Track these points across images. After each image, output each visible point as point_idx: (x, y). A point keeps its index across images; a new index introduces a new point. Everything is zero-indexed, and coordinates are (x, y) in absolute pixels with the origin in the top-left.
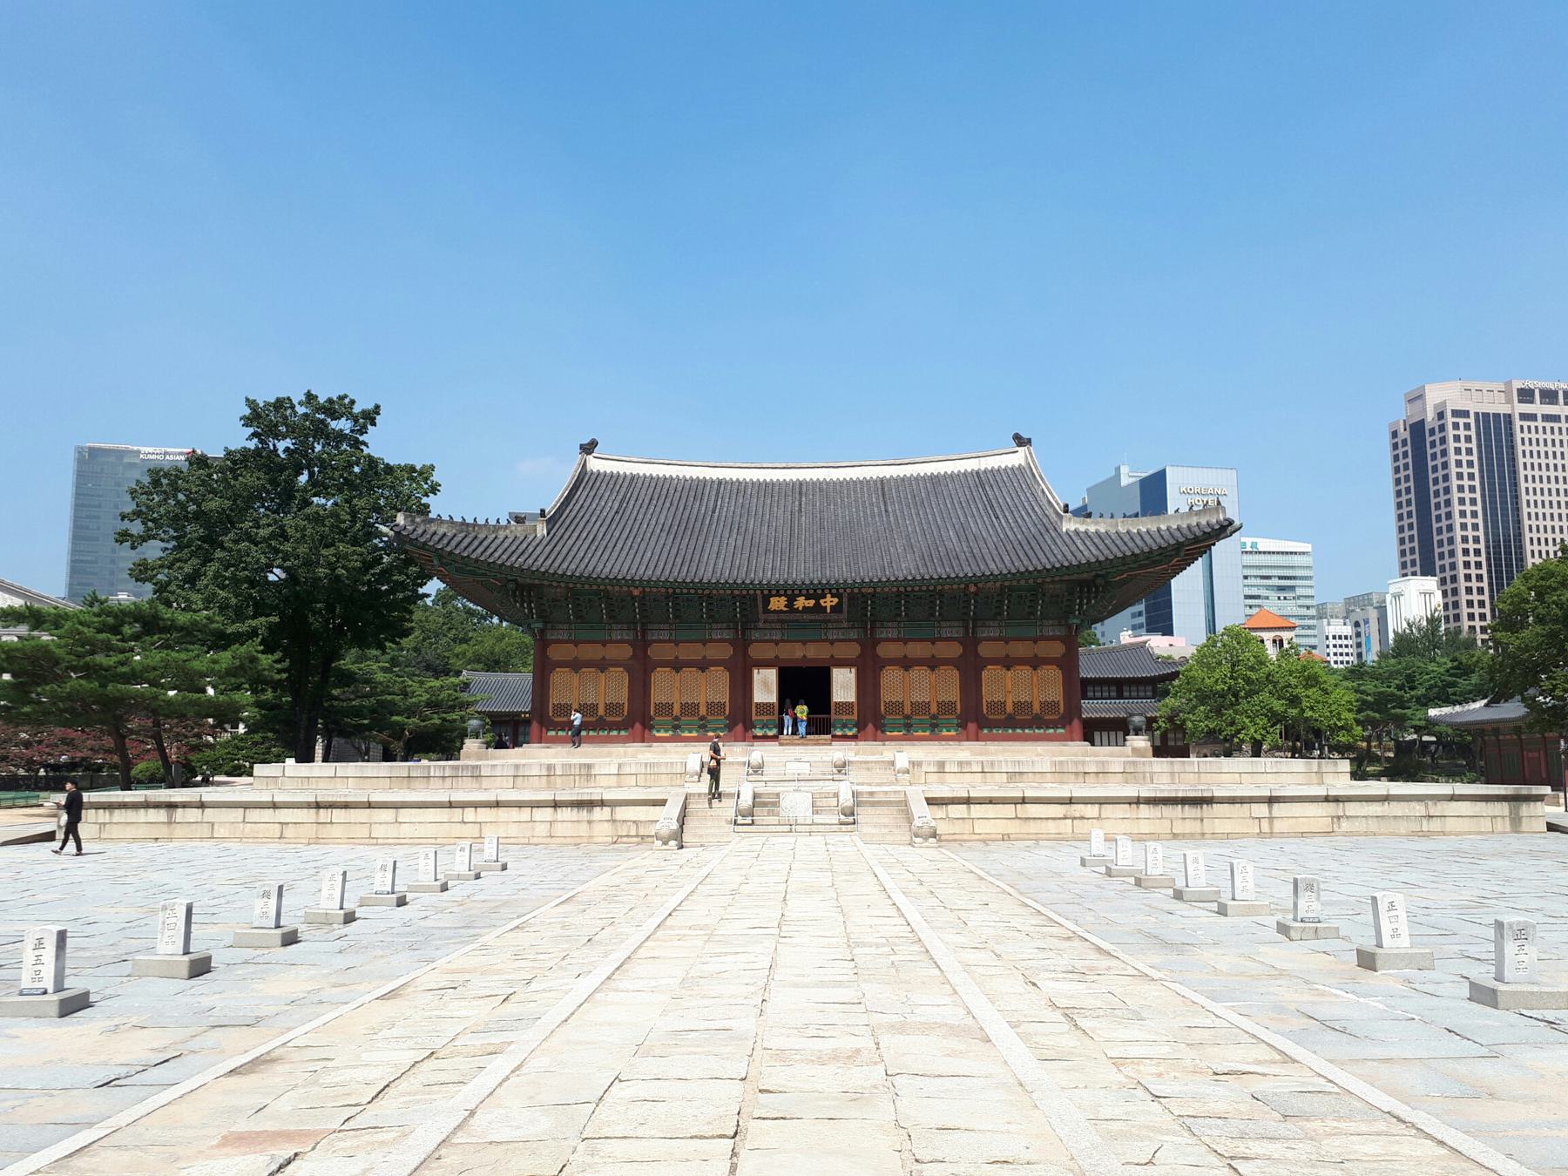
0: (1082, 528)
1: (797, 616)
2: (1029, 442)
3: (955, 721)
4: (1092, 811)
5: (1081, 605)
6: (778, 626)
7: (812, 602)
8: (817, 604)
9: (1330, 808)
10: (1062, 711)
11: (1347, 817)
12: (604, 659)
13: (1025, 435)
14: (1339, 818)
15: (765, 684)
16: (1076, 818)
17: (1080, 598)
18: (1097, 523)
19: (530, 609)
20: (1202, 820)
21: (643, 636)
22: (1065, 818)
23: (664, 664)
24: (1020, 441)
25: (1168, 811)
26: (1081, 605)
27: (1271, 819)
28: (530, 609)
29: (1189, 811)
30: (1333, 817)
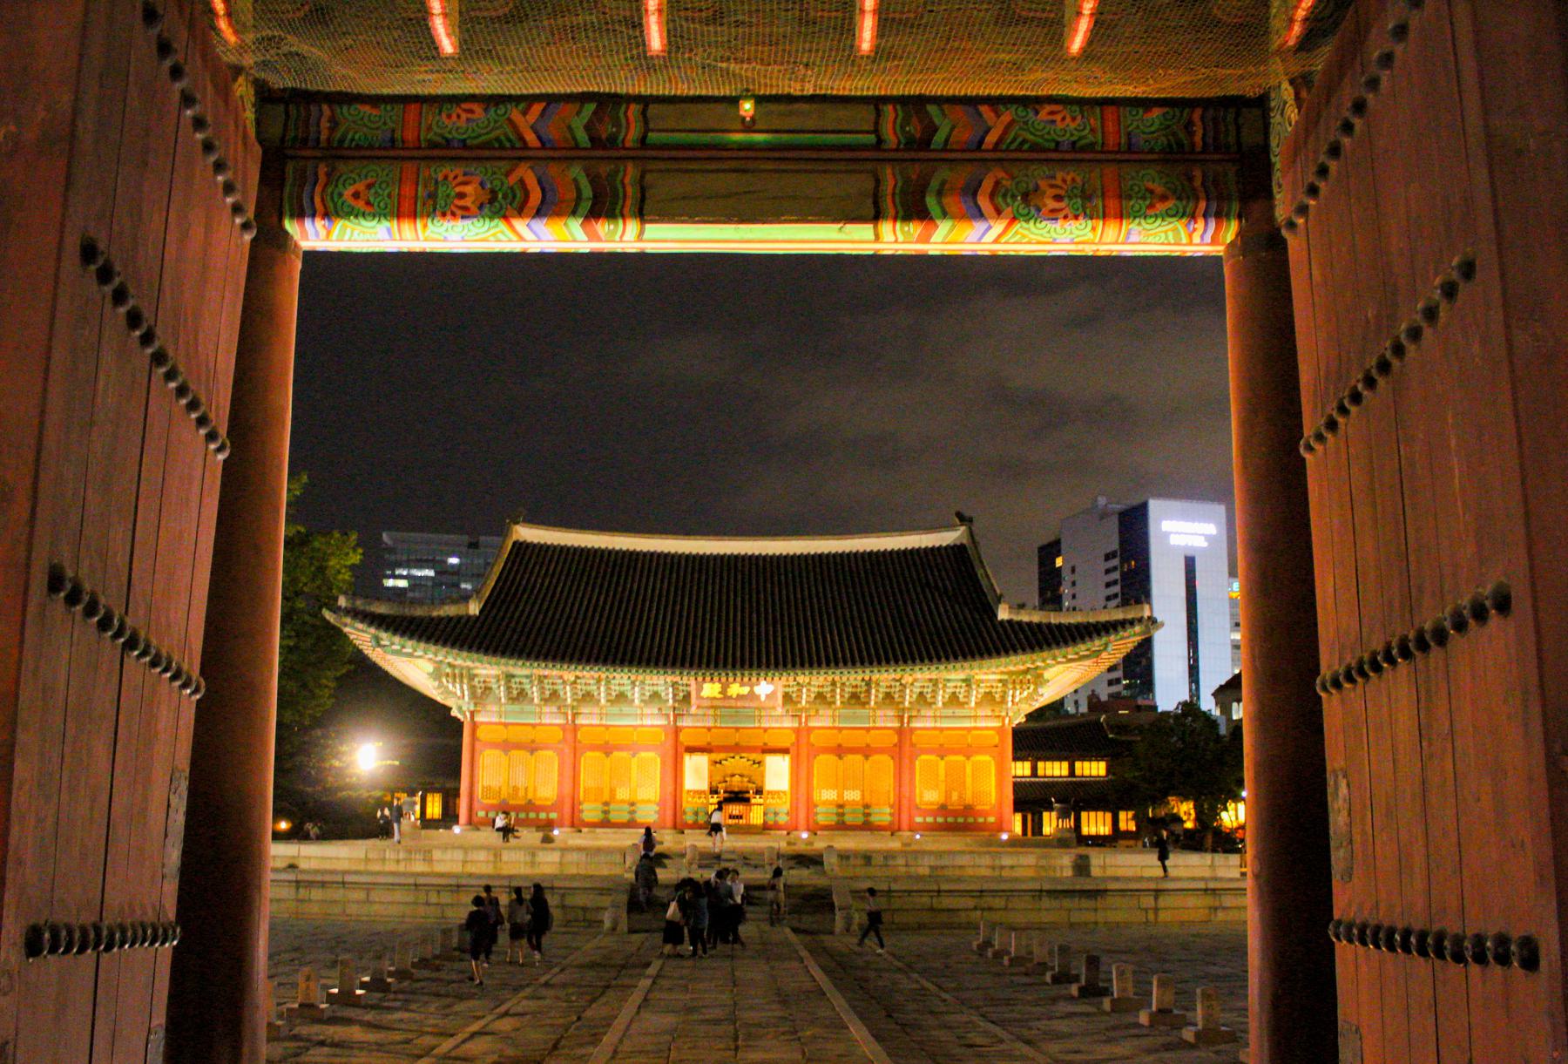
0: (1016, 618)
1: (733, 703)
2: (971, 520)
3: (888, 810)
4: (998, 902)
5: (1013, 696)
6: (711, 712)
7: (745, 690)
8: (752, 691)
9: (1208, 900)
10: (993, 801)
11: (1225, 909)
12: (533, 741)
13: (967, 514)
14: (1216, 909)
15: (697, 770)
16: (983, 910)
17: (1014, 688)
18: (1030, 614)
19: (463, 692)
20: (1096, 910)
21: (573, 721)
22: (975, 908)
23: (593, 748)
24: (963, 519)
25: (1067, 903)
26: (1013, 696)
27: (1156, 910)
28: (463, 692)
29: (1086, 903)
30: (1210, 908)
